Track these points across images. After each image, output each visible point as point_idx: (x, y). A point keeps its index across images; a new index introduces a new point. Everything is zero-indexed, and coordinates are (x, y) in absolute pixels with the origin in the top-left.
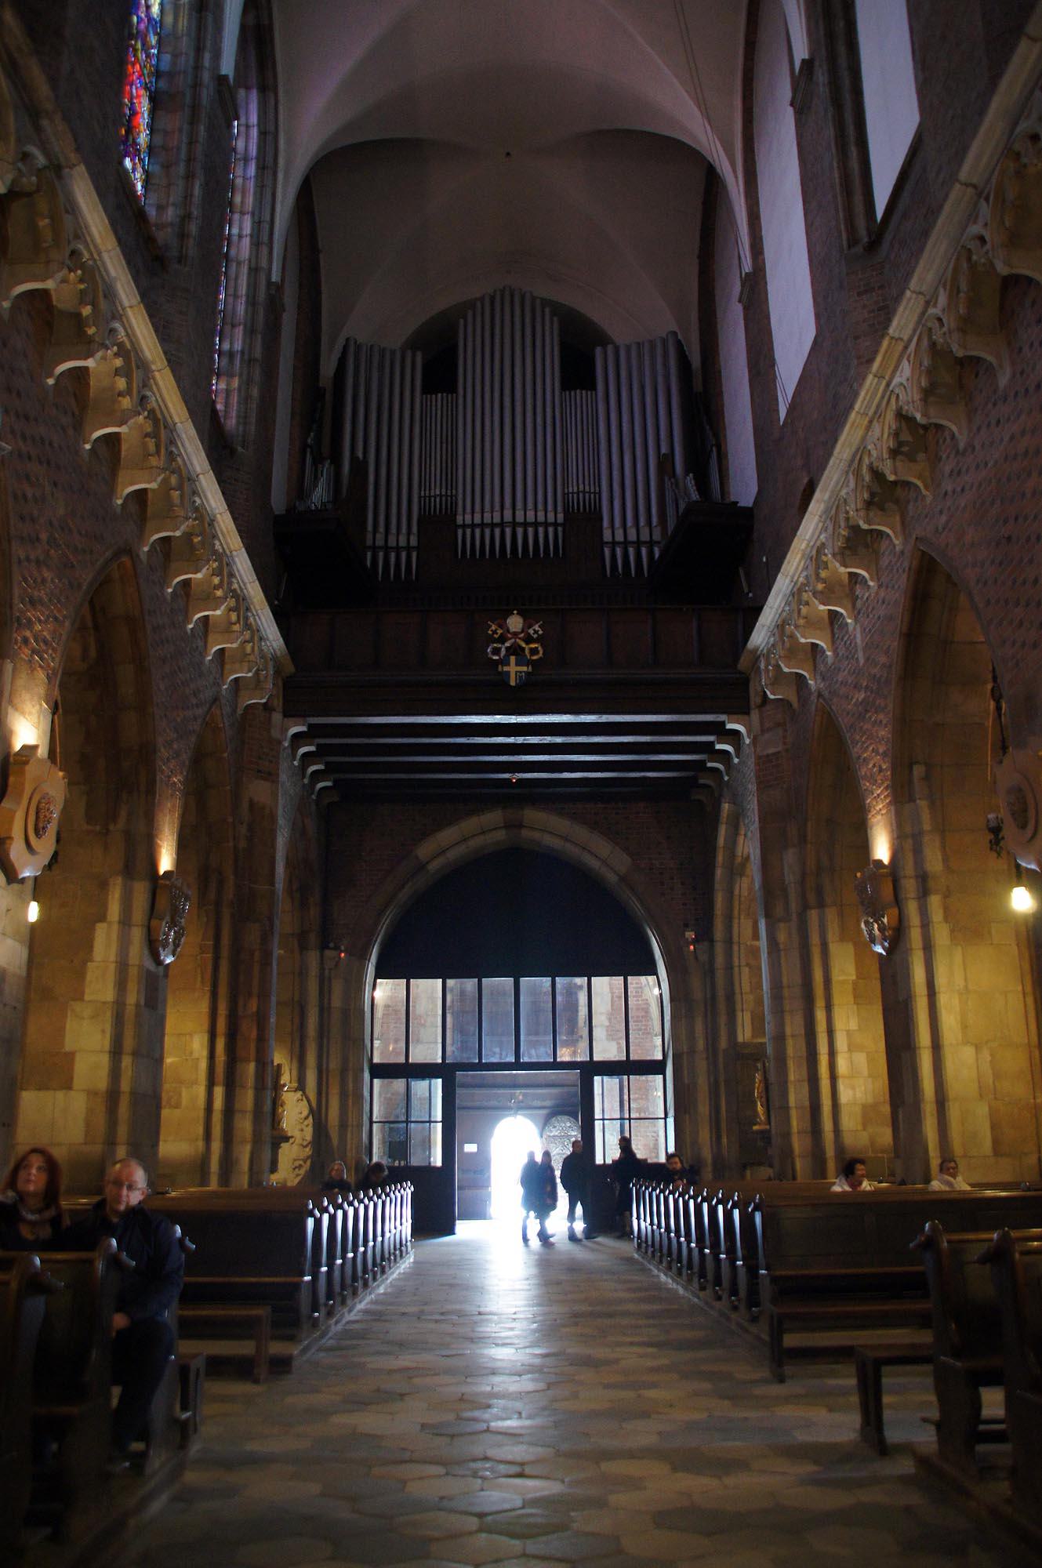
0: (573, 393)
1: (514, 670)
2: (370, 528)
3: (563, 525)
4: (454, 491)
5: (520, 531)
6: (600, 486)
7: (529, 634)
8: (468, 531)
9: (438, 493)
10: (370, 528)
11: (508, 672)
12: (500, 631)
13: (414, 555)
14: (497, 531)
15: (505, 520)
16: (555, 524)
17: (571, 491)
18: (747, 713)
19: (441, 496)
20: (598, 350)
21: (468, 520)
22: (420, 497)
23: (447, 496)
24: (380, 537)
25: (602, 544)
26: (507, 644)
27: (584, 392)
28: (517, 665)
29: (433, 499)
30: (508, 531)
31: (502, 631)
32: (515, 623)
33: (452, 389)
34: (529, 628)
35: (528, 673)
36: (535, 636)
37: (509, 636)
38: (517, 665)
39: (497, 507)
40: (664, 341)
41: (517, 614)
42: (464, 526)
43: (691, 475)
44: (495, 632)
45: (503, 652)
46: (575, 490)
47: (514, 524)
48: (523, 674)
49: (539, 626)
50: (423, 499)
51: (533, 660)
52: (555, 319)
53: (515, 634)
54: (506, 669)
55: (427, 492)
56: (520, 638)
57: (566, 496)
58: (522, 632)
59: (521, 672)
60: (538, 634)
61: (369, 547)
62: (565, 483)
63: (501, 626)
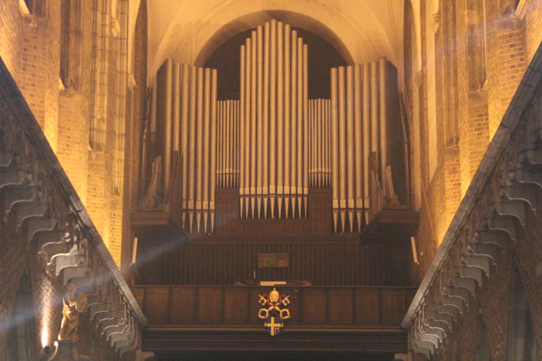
0: (316, 101)
1: (273, 326)
2: (184, 197)
3: (308, 196)
4: (238, 170)
5: (280, 200)
6: (332, 169)
7: (282, 303)
8: (247, 199)
9: (227, 172)
10: (184, 197)
11: (270, 328)
12: (265, 301)
13: (213, 215)
14: (266, 200)
15: (271, 193)
16: (303, 195)
17: (313, 171)
18: (406, 353)
19: (229, 174)
20: (334, 70)
21: (247, 193)
22: (216, 174)
23: (233, 173)
24: (191, 203)
25: (332, 209)
26: (271, 308)
27: (323, 100)
28: (275, 323)
29: (224, 176)
30: (272, 200)
31: (267, 301)
32: (275, 295)
33: (237, 98)
34: (283, 298)
35: (281, 328)
36: (286, 304)
37: (271, 304)
38: (275, 323)
39: (266, 183)
40: (378, 64)
41: (276, 290)
42: (244, 196)
43: (389, 167)
44: (263, 301)
45: (267, 314)
46: (316, 171)
47: (276, 195)
48: (278, 328)
49: (288, 298)
50: (218, 176)
51: (284, 320)
52: (306, 46)
53: (274, 303)
54: (269, 325)
55: (221, 171)
56: (277, 306)
57: (310, 175)
58: (279, 301)
59: (277, 327)
60: (287, 303)
61: (184, 210)
62: (310, 166)
63: (266, 298)
